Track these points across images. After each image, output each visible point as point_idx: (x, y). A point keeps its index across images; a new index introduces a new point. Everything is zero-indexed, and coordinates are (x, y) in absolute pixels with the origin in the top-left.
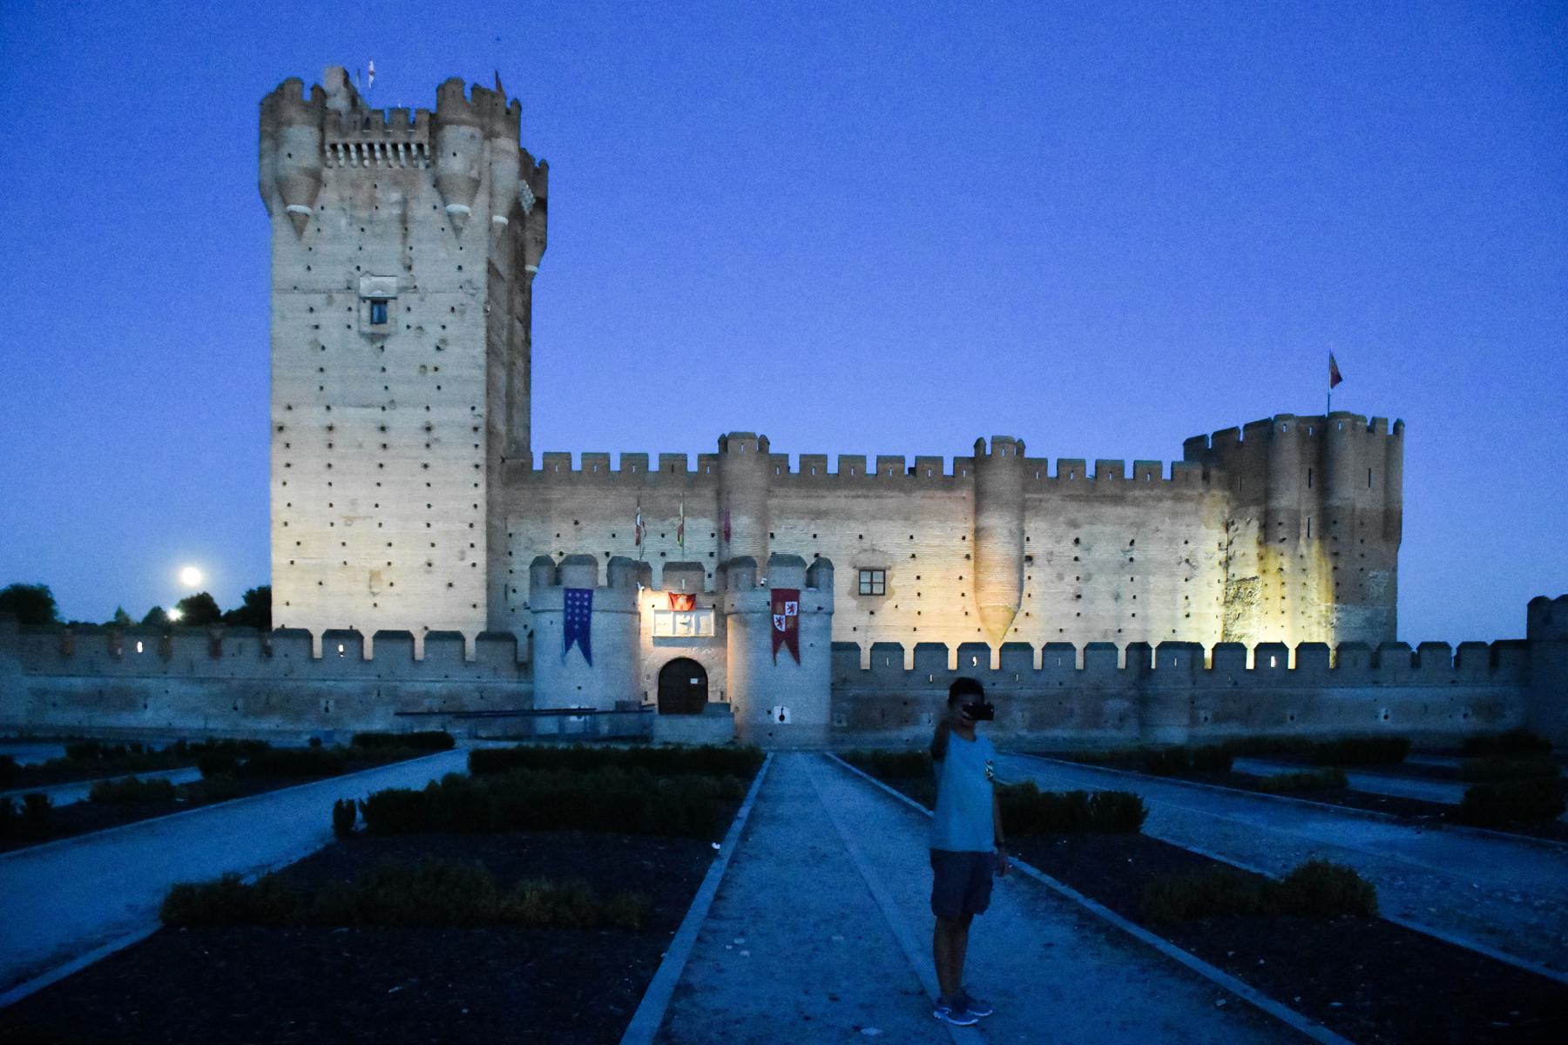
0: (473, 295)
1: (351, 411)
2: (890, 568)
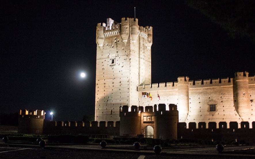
0: (128, 56)
1: (108, 80)
2: (216, 104)
